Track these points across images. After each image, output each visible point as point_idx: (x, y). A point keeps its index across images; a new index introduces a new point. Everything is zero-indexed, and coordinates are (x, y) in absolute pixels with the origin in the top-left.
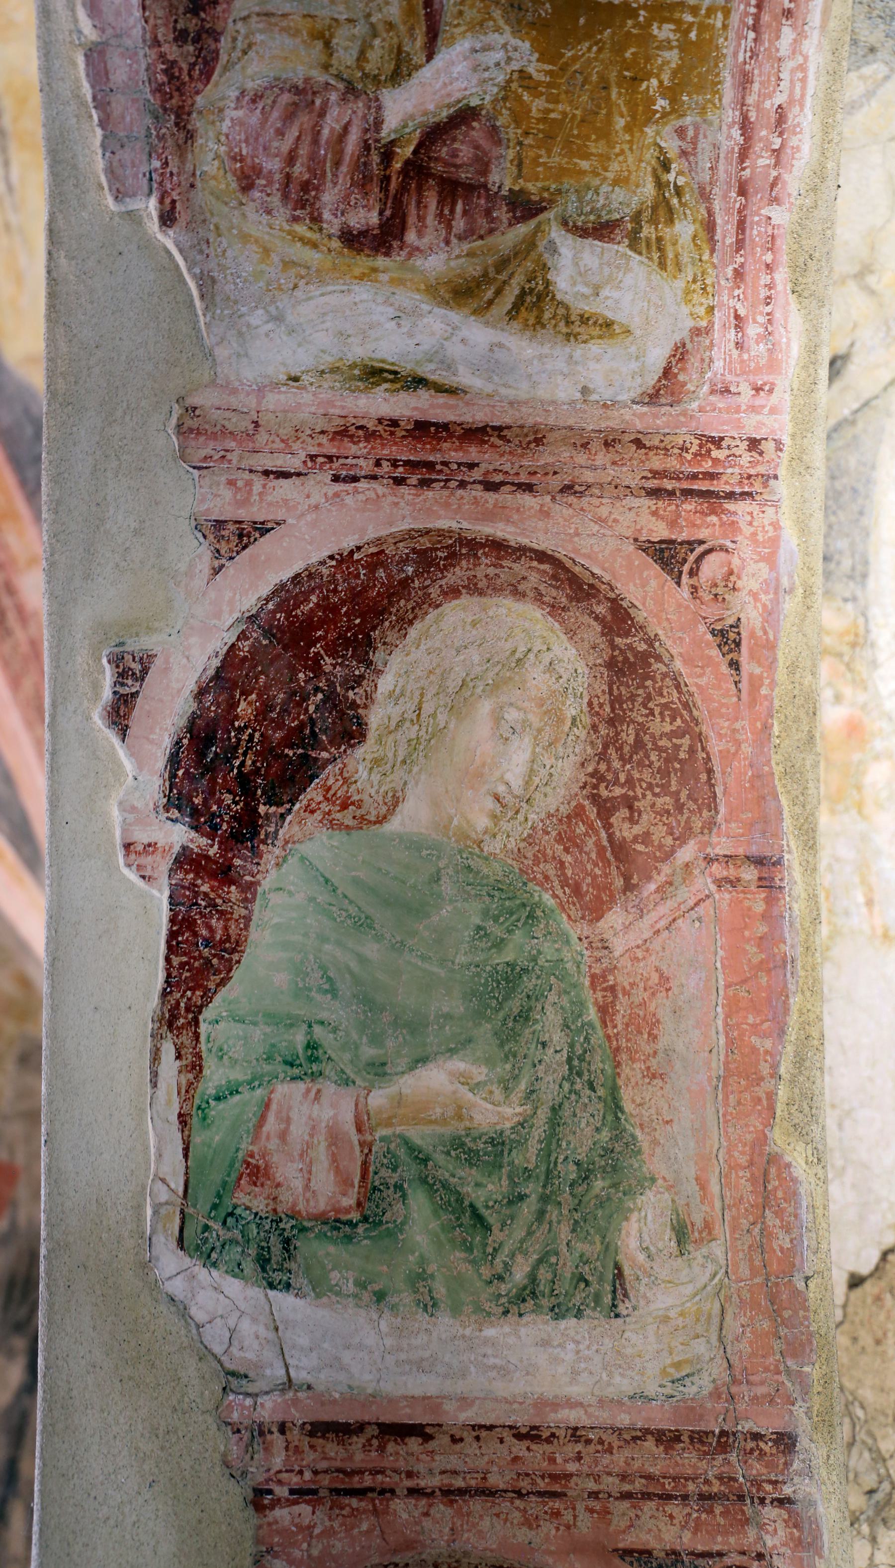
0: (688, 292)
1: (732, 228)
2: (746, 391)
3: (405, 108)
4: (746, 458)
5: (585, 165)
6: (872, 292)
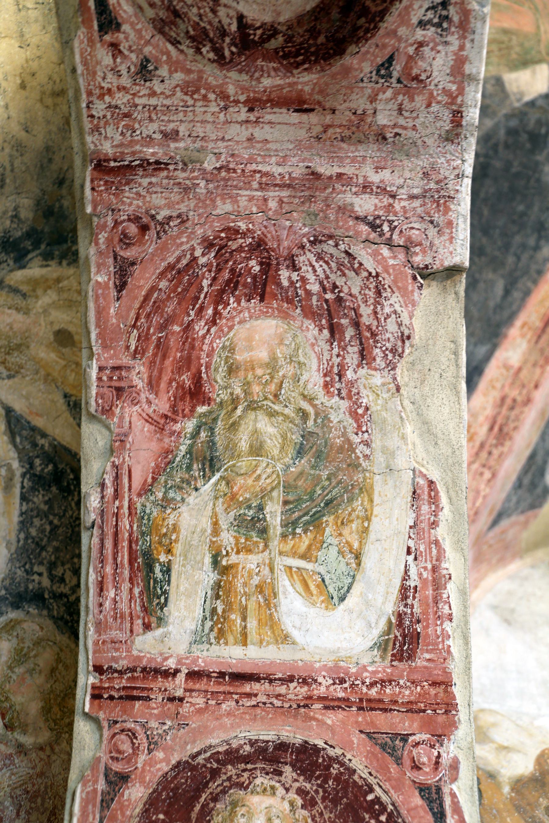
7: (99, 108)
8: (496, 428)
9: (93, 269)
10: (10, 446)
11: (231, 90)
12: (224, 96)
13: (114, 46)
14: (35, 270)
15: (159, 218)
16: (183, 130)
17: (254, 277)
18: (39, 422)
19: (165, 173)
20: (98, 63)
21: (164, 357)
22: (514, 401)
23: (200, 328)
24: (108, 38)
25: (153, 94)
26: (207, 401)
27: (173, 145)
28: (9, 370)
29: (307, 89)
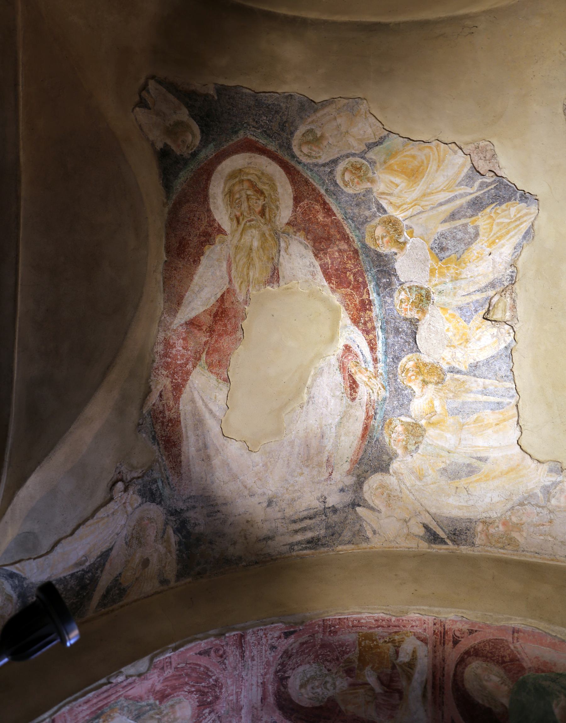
0: (407, 636)
1: (396, 628)
2: (425, 625)
3: (378, 689)
4: (437, 626)
5: (386, 656)
6: (410, 519)
7: (261, 633)
9: (206, 641)
10: (96, 558)
11: (268, 676)
12: (266, 674)
13: (280, 637)
14: (174, 539)
15: (225, 661)
16: (255, 662)
17: (206, 700)
18: (107, 566)
19: (240, 659)
20: (275, 632)
21: (176, 679)
23: (187, 688)
24: (282, 635)
25: (266, 651)
26: (161, 702)
27: (250, 660)
28: (129, 541)
29: (268, 700)
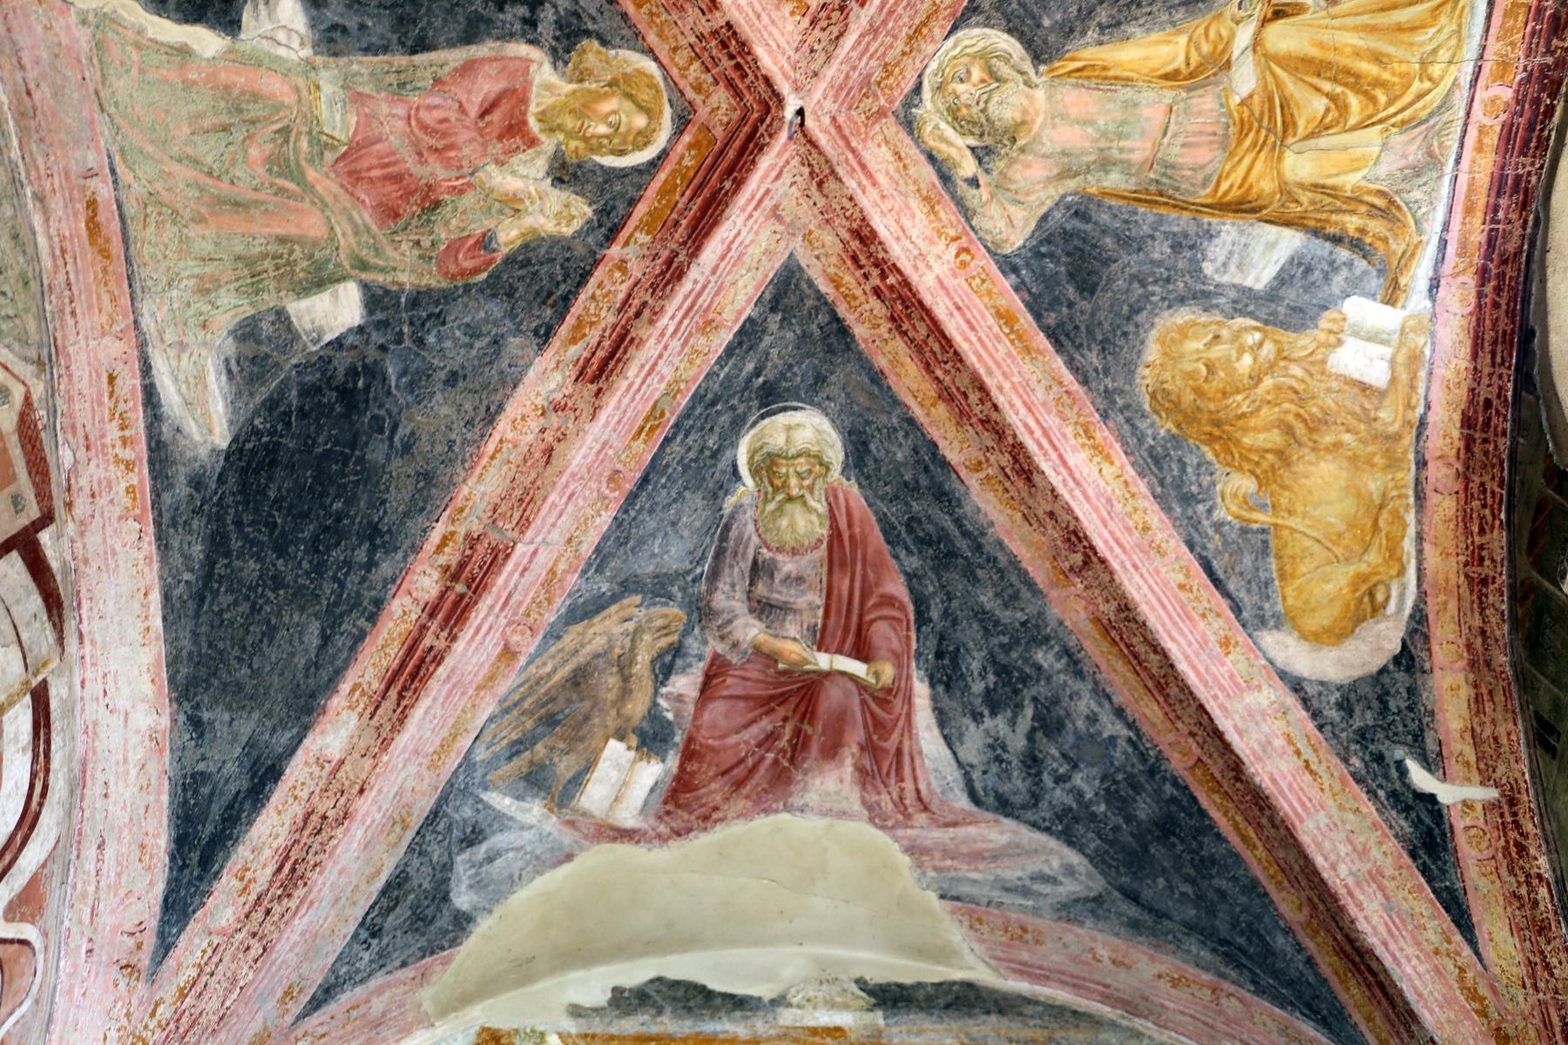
8: (287, 867)
22: (324, 817)
